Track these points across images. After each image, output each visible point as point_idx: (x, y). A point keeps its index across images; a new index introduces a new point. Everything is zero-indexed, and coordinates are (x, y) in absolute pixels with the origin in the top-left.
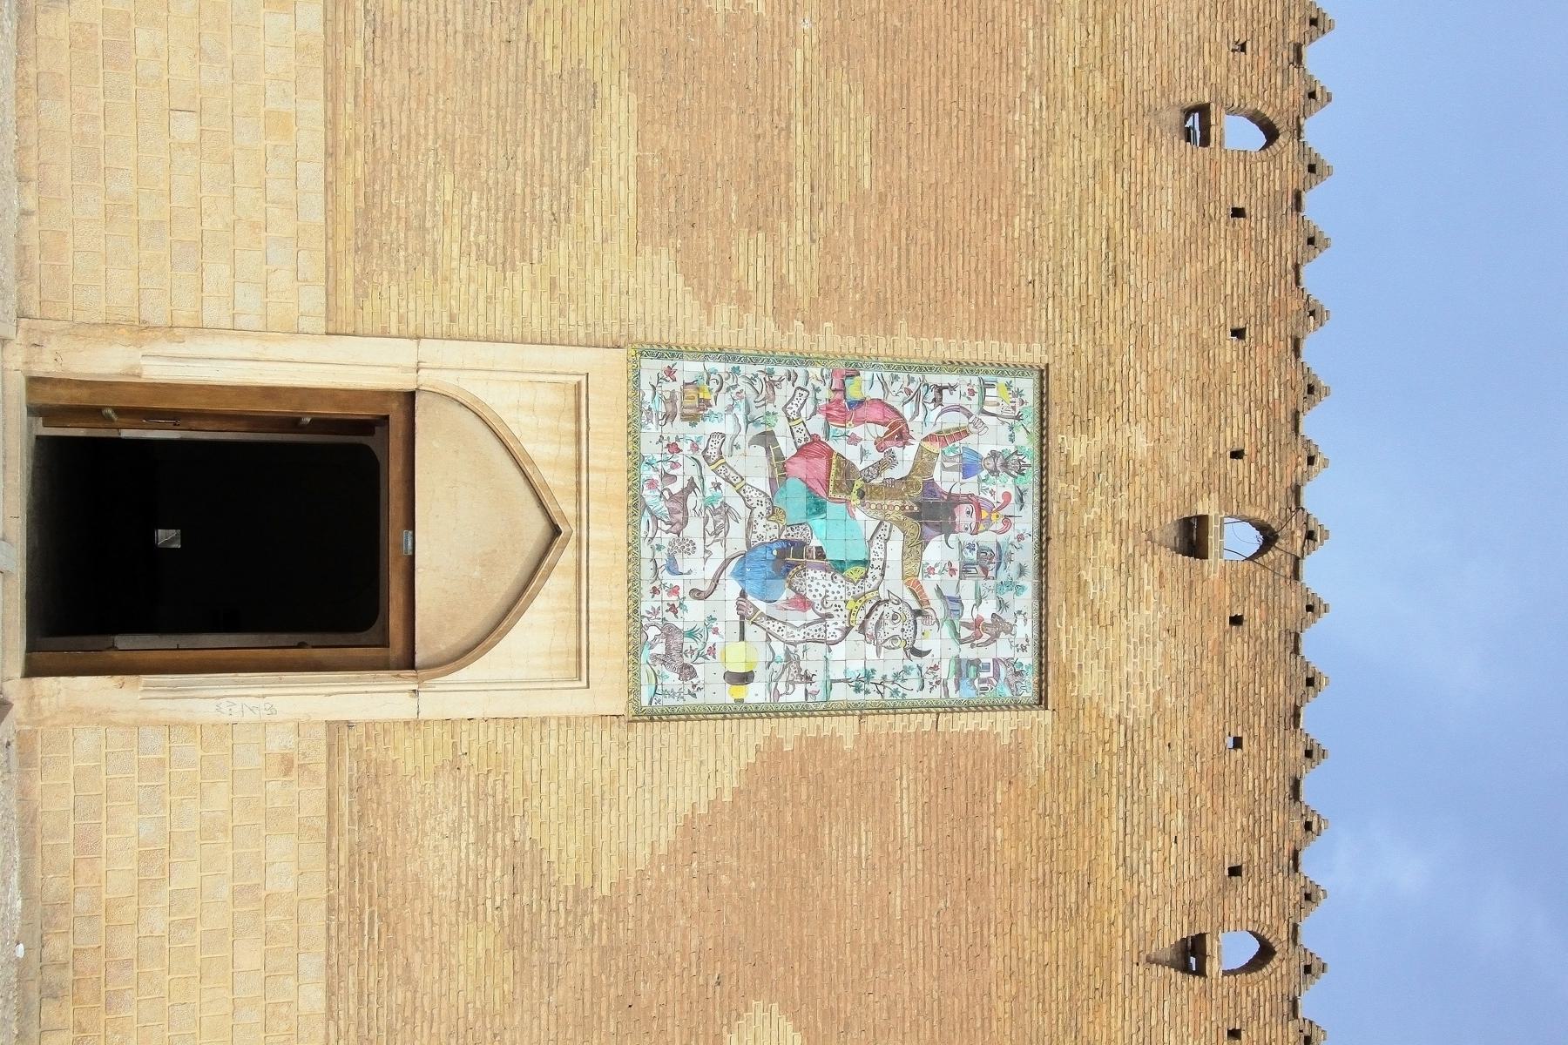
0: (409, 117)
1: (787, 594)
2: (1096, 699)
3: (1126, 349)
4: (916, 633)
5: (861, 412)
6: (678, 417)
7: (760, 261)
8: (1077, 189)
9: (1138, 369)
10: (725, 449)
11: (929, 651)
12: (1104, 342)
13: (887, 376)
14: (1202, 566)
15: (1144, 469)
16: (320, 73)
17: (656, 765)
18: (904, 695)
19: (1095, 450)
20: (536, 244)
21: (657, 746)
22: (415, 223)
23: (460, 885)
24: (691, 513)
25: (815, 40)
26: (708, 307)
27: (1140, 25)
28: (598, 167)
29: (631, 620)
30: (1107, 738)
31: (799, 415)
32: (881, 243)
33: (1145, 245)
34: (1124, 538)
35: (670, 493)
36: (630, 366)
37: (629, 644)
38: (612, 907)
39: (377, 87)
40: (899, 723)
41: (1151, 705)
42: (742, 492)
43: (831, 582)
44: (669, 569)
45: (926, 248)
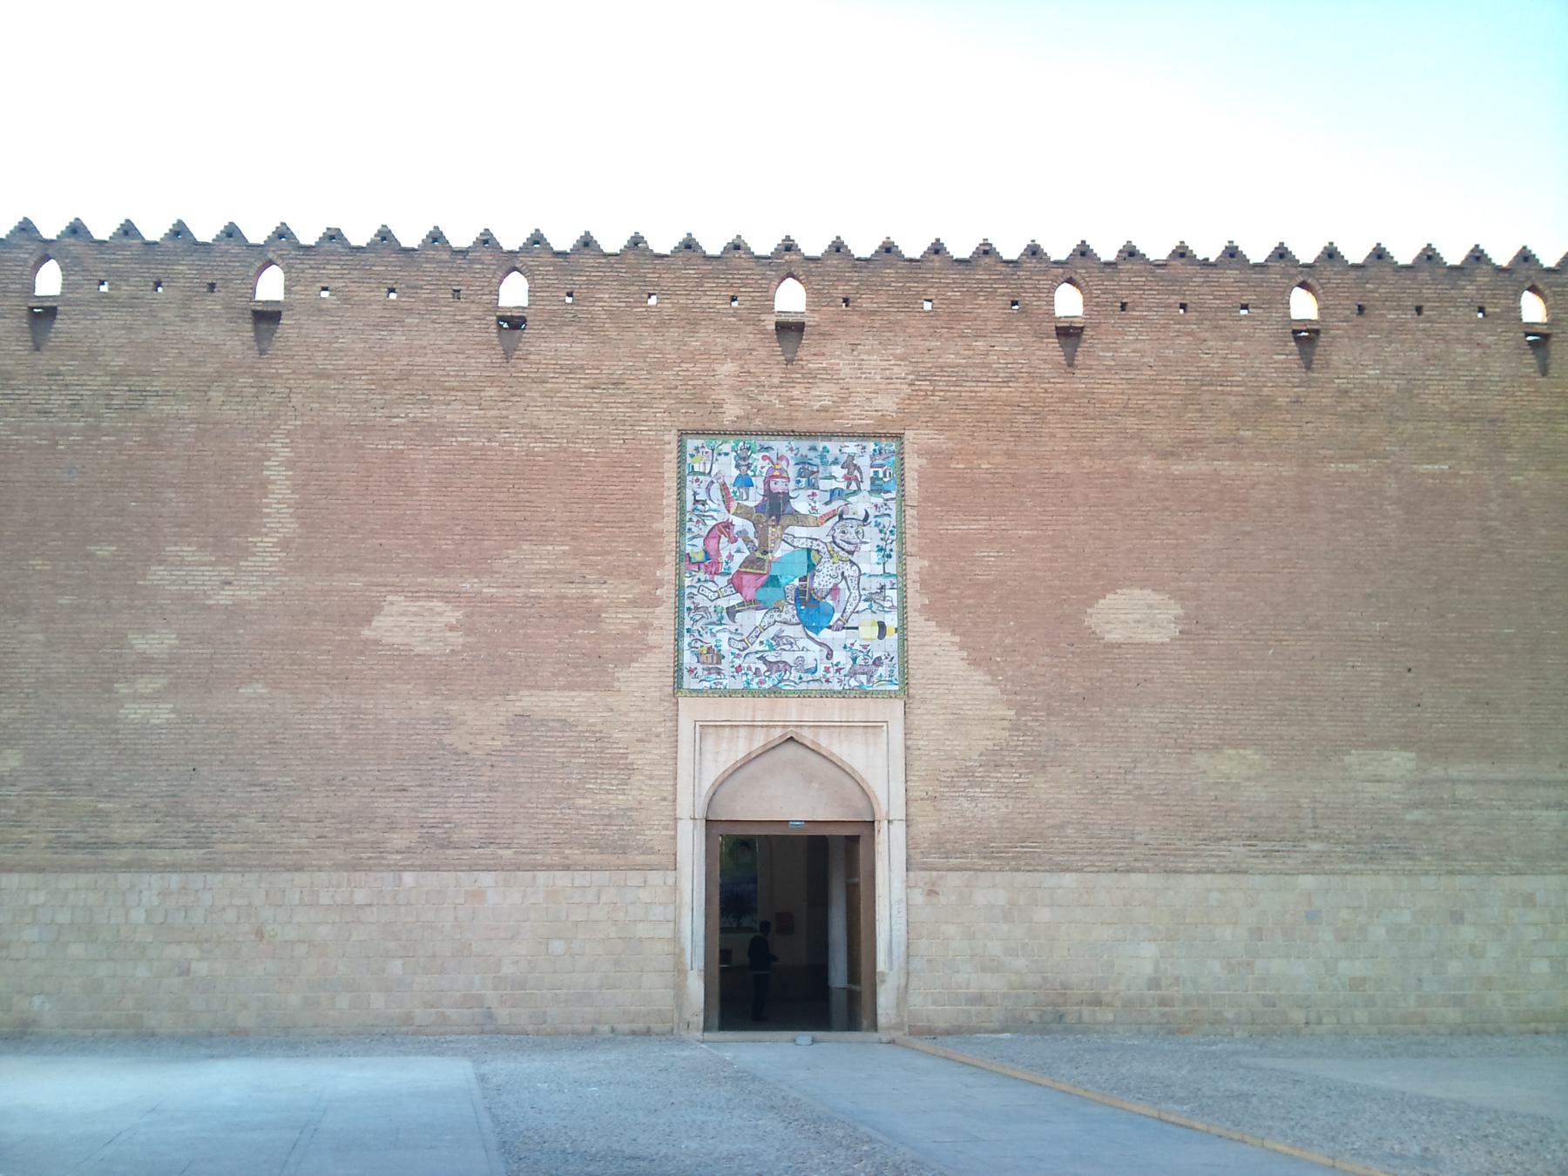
0: (542, 824)
1: (829, 600)
2: (897, 400)
3: (665, 377)
5: (712, 553)
7: (619, 616)
8: (561, 409)
10: (738, 638)
11: (867, 512)
12: (661, 392)
14: (810, 326)
16: (520, 873)
17: (935, 682)
19: (734, 400)
20: (616, 751)
21: (924, 681)
22: (606, 821)
23: (1005, 797)
24: (779, 659)
25: (476, 580)
26: (650, 648)
27: (447, 364)
28: (566, 714)
30: (923, 393)
32: (603, 539)
33: (596, 363)
38: (1023, 709)
39: (526, 842)
40: (911, 532)
41: (902, 363)
44: (813, 673)
45: (605, 510)
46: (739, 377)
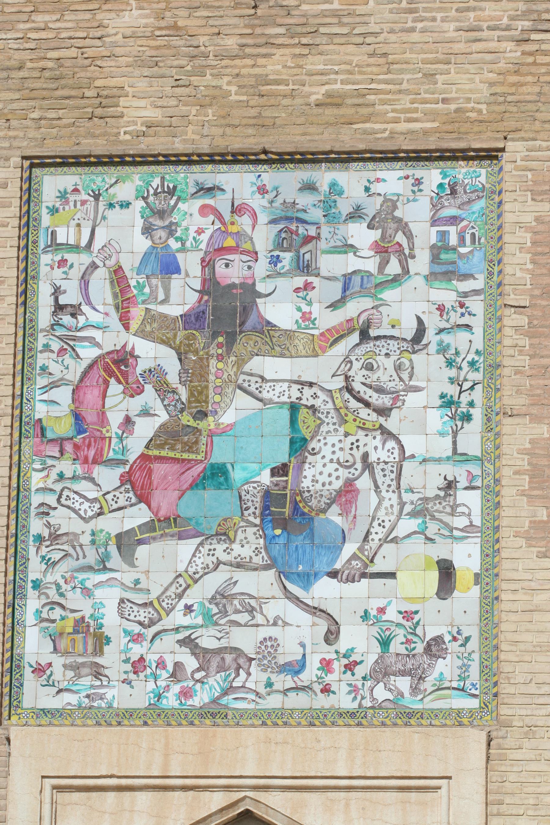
4: (392, 337)
5: (90, 417)
6: (98, 660)
9: (28, 26)
10: (140, 598)
13: (41, 381)
15: (168, 14)
18: (477, 352)
19: (142, 84)
21: (532, 689)
24: (224, 643)
29: (364, 721)
31: (96, 500)
34: (262, 40)
35: (198, 670)
36: (31, 722)
37: (395, 725)
42: (197, 576)
43: (319, 456)
44: (297, 673)
46: (153, 37)
